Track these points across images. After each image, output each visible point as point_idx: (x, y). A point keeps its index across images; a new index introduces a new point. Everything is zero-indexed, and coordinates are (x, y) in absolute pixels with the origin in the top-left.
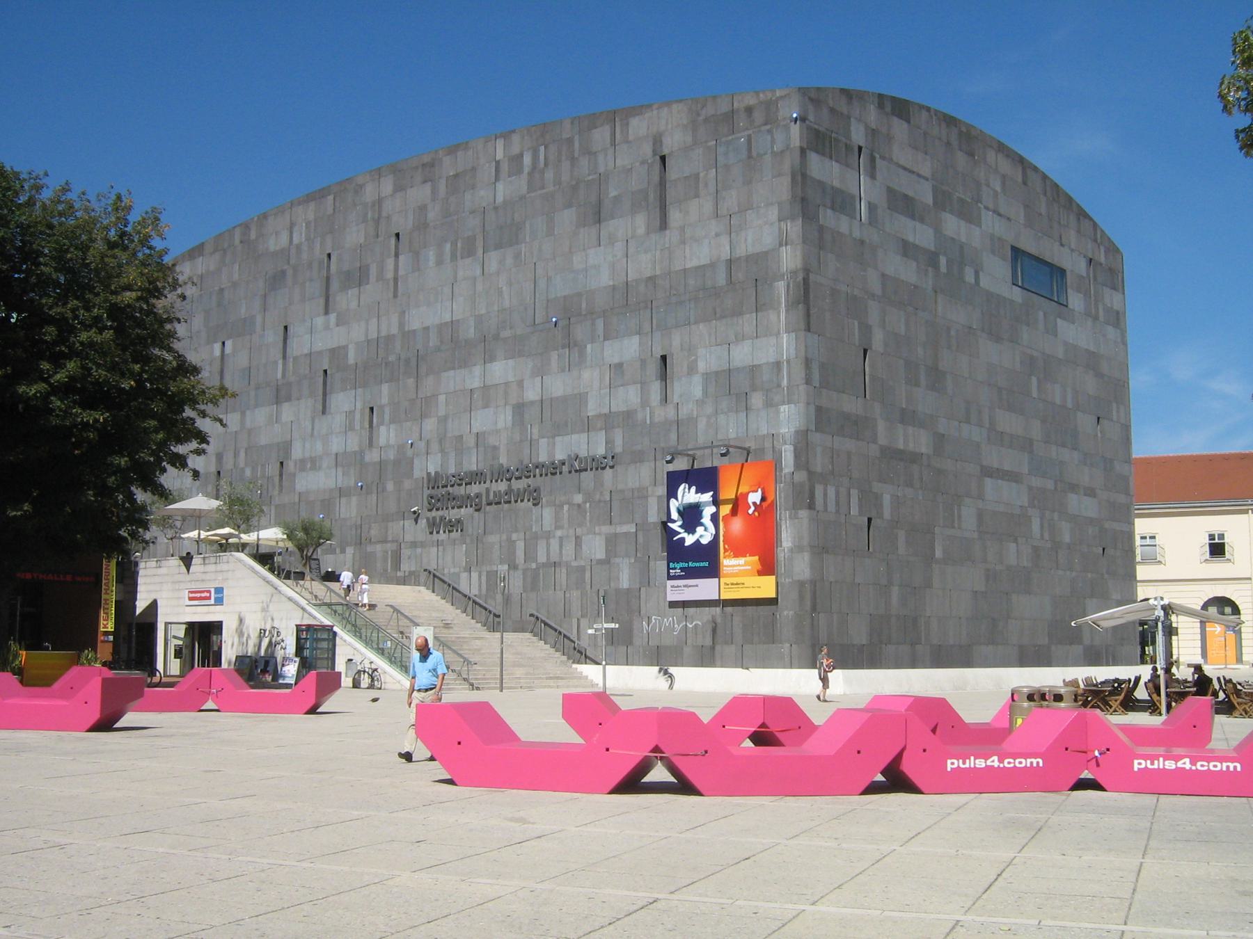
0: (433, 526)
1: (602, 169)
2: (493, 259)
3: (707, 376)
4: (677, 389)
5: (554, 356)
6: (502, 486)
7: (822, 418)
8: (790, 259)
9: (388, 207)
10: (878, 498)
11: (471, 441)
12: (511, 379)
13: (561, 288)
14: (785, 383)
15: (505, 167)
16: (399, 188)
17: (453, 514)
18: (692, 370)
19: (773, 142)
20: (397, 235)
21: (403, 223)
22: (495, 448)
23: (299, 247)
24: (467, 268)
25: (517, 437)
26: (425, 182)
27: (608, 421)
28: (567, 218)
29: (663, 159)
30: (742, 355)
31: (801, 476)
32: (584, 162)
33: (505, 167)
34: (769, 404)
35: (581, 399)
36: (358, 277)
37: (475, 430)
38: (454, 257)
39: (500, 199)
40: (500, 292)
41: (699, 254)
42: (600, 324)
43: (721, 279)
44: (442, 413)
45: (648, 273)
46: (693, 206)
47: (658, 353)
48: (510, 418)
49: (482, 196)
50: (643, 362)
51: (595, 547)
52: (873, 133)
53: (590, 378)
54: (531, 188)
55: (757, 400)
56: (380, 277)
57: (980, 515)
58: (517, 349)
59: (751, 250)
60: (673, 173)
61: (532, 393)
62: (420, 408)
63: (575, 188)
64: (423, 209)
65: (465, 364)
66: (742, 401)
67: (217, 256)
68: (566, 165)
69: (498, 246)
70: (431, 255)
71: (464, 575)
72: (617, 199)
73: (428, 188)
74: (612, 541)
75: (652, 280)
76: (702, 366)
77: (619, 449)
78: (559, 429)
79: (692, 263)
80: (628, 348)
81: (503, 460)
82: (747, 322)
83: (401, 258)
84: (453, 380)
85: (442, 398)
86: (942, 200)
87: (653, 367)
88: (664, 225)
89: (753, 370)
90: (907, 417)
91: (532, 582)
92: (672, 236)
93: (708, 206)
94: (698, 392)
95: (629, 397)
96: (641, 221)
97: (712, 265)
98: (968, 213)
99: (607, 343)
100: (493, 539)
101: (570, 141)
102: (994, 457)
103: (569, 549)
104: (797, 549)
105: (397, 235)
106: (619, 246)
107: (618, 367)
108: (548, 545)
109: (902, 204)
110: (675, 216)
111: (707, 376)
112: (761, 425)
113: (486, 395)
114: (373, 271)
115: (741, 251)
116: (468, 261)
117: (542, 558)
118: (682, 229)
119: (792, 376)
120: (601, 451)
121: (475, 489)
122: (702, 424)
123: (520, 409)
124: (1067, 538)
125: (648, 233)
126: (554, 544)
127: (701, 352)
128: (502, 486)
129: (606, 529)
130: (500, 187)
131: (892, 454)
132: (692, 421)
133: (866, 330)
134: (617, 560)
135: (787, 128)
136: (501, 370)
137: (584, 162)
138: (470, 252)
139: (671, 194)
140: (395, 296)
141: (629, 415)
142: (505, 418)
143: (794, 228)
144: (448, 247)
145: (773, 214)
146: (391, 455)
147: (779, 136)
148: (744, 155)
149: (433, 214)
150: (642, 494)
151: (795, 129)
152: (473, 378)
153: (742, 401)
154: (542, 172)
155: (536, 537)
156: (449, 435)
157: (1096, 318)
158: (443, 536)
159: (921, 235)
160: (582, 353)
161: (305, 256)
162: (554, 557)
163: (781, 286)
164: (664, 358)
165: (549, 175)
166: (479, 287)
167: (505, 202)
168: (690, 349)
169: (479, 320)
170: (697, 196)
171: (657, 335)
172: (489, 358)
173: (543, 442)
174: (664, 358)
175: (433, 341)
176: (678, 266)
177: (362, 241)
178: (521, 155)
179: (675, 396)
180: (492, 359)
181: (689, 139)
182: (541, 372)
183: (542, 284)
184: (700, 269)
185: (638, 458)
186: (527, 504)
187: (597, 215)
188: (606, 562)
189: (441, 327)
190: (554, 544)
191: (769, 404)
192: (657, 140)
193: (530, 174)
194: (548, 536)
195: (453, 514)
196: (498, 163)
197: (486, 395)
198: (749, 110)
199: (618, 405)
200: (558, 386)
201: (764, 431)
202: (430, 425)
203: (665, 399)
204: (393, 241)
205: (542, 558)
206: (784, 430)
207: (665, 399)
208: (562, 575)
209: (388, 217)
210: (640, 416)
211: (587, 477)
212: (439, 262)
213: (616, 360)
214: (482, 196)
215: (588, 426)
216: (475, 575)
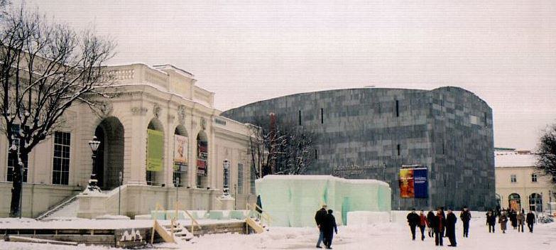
2: (351, 118)
4: (402, 152)
5: (369, 143)
7: (437, 160)
10: (446, 176)
12: (357, 146)
24: (344, 119)
27: (384, 158)
30: (418, 146)
33: (353, 97)
34: (425, 157)
36: (311, 118)
38: (340, 116)
41: (406, 124)
42: (381, 136)
44: (337, 153)
54: (361, 103)
55: (422, 156)
56: (318, 117)
57: (464, 178)
58: (358, 139)
60: (400, 105)
61: (363, 150)
62: (332, 152)
63: (373, 104)
64: (329, 104)
66: (418, 156)
69: (353, 115)
70: (333, 116)
75: (395, 128)
76: (407, 150)
78: (372, 158)
79: (405, 125)
80: (389, 142)
82: (420, 140)
83: (324, 115)
84: (340, 145)
85: (337, 150)
86: (456, 108)
87: (395, 147)
88: (398, 115)
90: (451, 158)
92: (400, 118)
93: (409, 113)
94: (407, 153)
95: (389, 153)
96: (391, 115)
97: (411, 126)
98: (461, 109)
102: (466, 164)
104: (433, 187)
106: (385, 119)
107: (386, 146)
109: (449, 110)
110: (401, 114)
111: (409, 150)
112: (423, 161)
113: (350, 150)
114: (315, 117)
115: (417, 123)
123: (360, 154)
124: (480, 182)
131: (448, 166)
133: (443, 140)
136: (354, 144)
138: (344, 115)
139: (399, 109)
140: (322, 122)
144: (337, 114)
146: (322, 162)
149: (333, 105)
152: (346, 145)
153: (418, 156)
159: (452, 116)
161: (292, 111)
164: (399, 146)
168: (405, 144)
169: (348, 132)
172: (350, 141)
175: (334, 136)
178: (358, 95)
179: (401, 153)
182: (366, 146)
184: (407, 127)
187: (379, 111)
189: (336, 133)
191: (425, 157)
192: (395, 96)
193: (361, 100)
197: (350, 150)
199: (386, 155)
200: (370, 149)
202: (334, 156)
203: (399, 154)
207: (399, 154)
212: (335, 116)
215: (378, 158)
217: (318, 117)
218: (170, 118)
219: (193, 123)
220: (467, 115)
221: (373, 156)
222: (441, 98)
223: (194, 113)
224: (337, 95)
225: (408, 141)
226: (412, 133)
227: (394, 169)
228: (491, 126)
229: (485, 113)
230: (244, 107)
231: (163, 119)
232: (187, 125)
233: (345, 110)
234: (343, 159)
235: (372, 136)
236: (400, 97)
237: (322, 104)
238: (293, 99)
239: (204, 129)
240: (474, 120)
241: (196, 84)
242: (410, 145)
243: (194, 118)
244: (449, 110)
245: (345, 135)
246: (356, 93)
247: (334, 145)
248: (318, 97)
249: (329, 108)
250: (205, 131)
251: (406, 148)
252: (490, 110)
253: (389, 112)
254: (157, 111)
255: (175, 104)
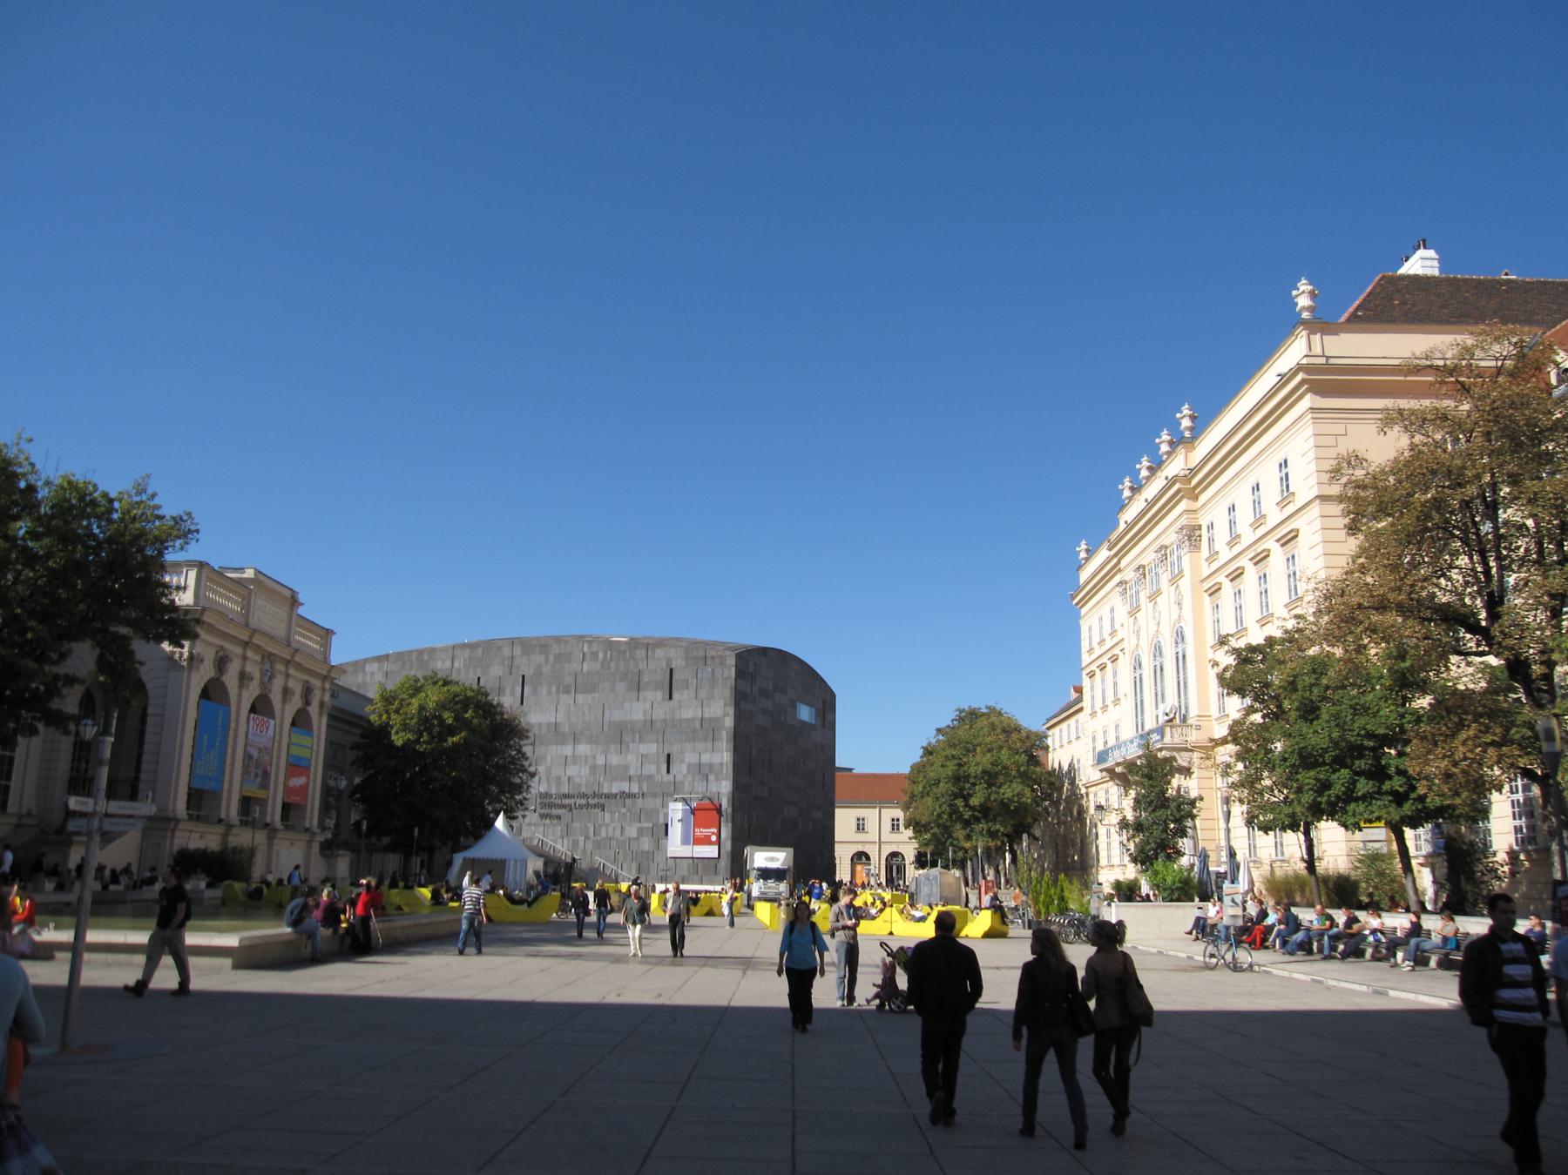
0: (543, 816)
1: (640, 667)
2: (581, 698)
3: (689, 765)
4: (674, 769)
6: (583, 801)
8: (729, 722)
9: (517, 662)
11: (566, 779)
12: (589, 753)
13: (617, 716)
14: (725, 771)
15: (588, 656)
16: (524, 653)
17: (555, 812)
18: (682, 761)
19: (723, 673)
20: (523, 677)
21: (529, 673)
22: (580, 785)
23: (459, 670)
24: (566, 699)
25: (592, 780)
26: (541, 653)
27: (640, 778)
28: (621, 687)
29: (671, 670)
30: (706, 758)
31: (730, 810)
32: (632, 663)
34: (717, 779)
35: (627, 767)
37: (568, 774)
38: (557, 693)
39: (585, 670)
40: (584, 714)
41: (690, 712)
42: (637, 736)
43: (697, 725)
45: (662, 717)
46: (686, 692)
47: (666, 752)
48: (588, 771)
49: (575, 666)
50: (658, 754)
51: (632, 832)
52: (756, 664)
53: (631, 759)
55: (712, 777)
56: (512, 694)
58: (591, 741)
59: (711, 716)
61: (601, 761)
64: (540, 666)
65: (563, 743)
67: (400, 663)
68: (622, 663)
69: (584, 692)
70: (545, 690)
71: (560, 841)
72: (648, 683)
73: (543, 657)
74: (640, 830)
75: (664, 721)
76: (687, 760)
77: (645, 790)
79: (684, 717)
80: (651, 748)
81: (584, 790)
85: (549, 758)
87: (663, 759)
88: (671, 698)
89: (711, 766)
91: (598, 846)
94: (685, 771)
95: (650, 769)
96: (659, 695)
97: (694, 719)
99: (641, 745)
100: (576, 825)
101: (624, 652)
103: (618, 832)
105: (523, 677)
106: (648, 705)
108: (607, 830)
109: (765, 693)
110: (676, 695)
111: (689, 765)
112: (713, 788)
113: (575, 759)
114: (508, 691)
115: (706, 715)
116: (566, 696)
117: (603, 834)
118: (680, 702)
119: (728, 769)
120: (635, 789)
121: (566, 802)
122: (686, 784)
123: (594, 768)
125: (663, 700)
126: (610, 829)
127: (687, 754)
128: (583, 801)
129: (638, 825)
130: (585, 664)
132: (682, 783)
134: (644, 839)
135: (730, 669)
136: (583, 749)
137: (632, 663)
138: (567, 691)
141: (650, 778)
142: (585, 771)
143: (731, 710)
144: (554, 688)
145: (722, 703)
147: (726, 672)
148: (710, 676)
150: (657, 812)
151: (733, 670)
152: (568, 750)
154: (609, 663)
155: (600, 825)
156: (553, 775)
157: (824, 726)
158: (548, 821)
160: (628, 747)
162: (610, 835)
163: (724, 734)
164: (669, 755)
165: (613, 665)
166: (572, 709)
167: (588, 673)
168: (682, 752)
170: (687, 688)
171: (666, 744)
172: (576, 741)
173: (606, 785)
174: (669, 755)
175: (544, 730)
176: (677, 717)
177: (501, 674)
180: (579, 743)
181: (684, 664)
183: (607, 713)
184: (688, 720)
185: (654, 795)
186: (597, 811)
188: (638, 839)
189: (549, 724)
190: (610, 829)
192: (669, 661)
194: (607, 826)
195: (555, 812)
196: (584, 654)
197: (575, 759)
198: (713, 657)
200: (614, 760)
201: (714, 790)
203: (668, 771)
204: (521, 679)
205: (603, 834)
206: (723, 791)
207: (668, 771)
208: (614, 843)
209: (518, 667)
210: (656, 779)
211: (628, 801)
212: (549, 693)
213: (645, 752)
214: (575, 666)
216: (565, 841)
217: (512, 694)
218: (244, 677)
219: (286, 692)
220: (794, 707)
221: (622, 773)
222: (751, 669)
223: (292, 671)
224: (556, 649)
225: (688, 745)
226: (695, 731)
227: (659, 801)
228: (832, 727)
229: (824, 702)
230: (366, 660)
231: (231, 679)
232: (276, 697)
233: (569, 680)
234: (559, 778)
235: (621, 735)
236: (678, 663)
237: (526, 666)
238: (467, 652)
239: (308, 703)
240: (805, 713)
241: (301, 611)
242: (688, 756)
243: (291, 684)
244: (765, 693)
245: (567, 729)
246: (595, 648)
247: (542, 748)
248: (518, 651)
249: (538, 674)
250: (309, 708)
251: (682, 761)
252: (833, 695)
253: (656, 689)
254: (221, 663)
255: (258, 648)
